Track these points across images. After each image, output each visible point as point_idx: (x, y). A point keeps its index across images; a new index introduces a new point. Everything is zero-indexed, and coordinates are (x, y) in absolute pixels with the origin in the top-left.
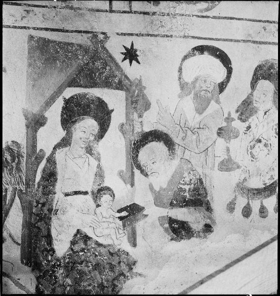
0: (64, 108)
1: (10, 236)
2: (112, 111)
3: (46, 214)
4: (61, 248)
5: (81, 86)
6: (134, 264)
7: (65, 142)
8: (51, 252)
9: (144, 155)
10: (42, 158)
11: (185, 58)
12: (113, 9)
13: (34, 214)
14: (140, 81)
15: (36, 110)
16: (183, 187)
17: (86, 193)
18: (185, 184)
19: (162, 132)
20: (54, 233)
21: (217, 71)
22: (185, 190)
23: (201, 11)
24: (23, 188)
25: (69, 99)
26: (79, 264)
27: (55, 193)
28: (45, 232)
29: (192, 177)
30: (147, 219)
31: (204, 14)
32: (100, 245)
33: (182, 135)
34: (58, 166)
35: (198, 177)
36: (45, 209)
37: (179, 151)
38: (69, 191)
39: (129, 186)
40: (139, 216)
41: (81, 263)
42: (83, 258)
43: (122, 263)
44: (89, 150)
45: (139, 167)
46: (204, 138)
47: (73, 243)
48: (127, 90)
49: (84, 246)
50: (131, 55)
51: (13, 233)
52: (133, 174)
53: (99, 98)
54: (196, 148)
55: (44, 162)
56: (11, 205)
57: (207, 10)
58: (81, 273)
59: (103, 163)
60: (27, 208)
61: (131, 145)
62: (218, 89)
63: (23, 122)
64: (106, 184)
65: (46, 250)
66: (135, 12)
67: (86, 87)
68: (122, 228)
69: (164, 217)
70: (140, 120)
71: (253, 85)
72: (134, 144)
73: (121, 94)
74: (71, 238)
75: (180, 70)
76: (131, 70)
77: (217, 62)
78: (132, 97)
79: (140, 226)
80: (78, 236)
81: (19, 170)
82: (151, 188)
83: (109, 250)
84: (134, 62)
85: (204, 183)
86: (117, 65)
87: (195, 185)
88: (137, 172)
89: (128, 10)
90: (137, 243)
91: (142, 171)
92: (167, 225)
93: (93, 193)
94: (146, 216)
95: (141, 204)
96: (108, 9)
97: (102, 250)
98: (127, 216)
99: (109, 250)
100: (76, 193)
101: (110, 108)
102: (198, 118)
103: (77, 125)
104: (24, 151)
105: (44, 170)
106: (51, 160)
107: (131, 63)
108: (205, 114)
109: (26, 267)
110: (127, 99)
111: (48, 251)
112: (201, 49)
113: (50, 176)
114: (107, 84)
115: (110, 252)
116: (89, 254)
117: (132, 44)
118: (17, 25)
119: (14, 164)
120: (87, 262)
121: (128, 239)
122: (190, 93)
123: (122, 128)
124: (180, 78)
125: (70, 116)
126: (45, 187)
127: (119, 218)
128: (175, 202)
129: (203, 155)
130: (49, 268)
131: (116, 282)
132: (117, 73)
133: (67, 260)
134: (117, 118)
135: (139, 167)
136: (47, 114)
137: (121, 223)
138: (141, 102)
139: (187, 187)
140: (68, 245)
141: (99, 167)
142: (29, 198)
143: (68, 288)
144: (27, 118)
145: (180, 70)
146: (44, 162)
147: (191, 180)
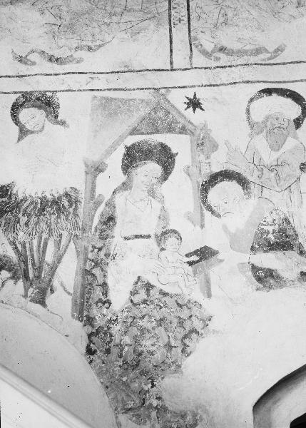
0: (125, 155)
1: (62, 285)
2: (177, 154)
3: (102, 260)
4: (119, 297)
5: (142, 134)
6: (210, 320)
7: (125, 186)
8: (107, 305)
9: (214, 195)
10: (98, 204)
11: (252, 100)
12: (174, 68)
13: (90, 260)
14: (205, 125)
15: (95, 158)
16: (265, 228)
17: (149, 236)
18: (268, 224)
19: (233, 172)
20: (110, 281)
22: (268, 233)
23: (264, 60)
24: (79, 233)
25: (130, 147)
26: (140, 318)
27: (113, 237)
28: (100, 281)
29: (274, 216)
30: (222, 265)
32: (165, 294)
33: (257, 173)
34: (117, 210)
35: (282, 216)
36: (102, 254)
37: (255, 190)
38: (129, 234)
39: (198, 228)
40: (213, 259)
41: (143, 317)
42: (145, 311)
43: (193, 318)
44: (152, 193)
45: (210, 208)
46: (284, 176)
47: (134, 293)
49: (145, 297)
50: (194, 104)
51: (65, 283)
52: (202, 215)
53: (162, 144)
54: (276, 185)
55: (103, 205)
56: (65, 251)
57: (270, 59)
58: (143, 330)
59: (167, 205)
60: (82, 254)
61: (199, 187)
62: (292, 124)
63: (83, 168)
64: (171, 227)
65: (100, 300)
66: (196, 68)
68: (192, 274)
69: (242, 264)
70: (208, 161)
72: (203, 185)
73: (185, 138)
74: (131, 288)
75: (248, 111)
76: (195, 117)
77: (289, 100)
78: (198, 139)
79: (215, 271)
80: (139, 284)
81: (76, 215)
82: (225, 228)
83: (176, 301)
84: (198, 110)
85: (292, 222)
86: (179, 113)
87: (279, 225)
88: (207, 214)
90: (212, 293)
91: (213, 212)
92: (250, 274)
93: (156, 236)
94: (221, 261)
95: (215, 248)
97: (167, 299)
98: (198, 262)
99: (176, 301)
100: (137, 237)
101: (174, 151)
102: (275, 155)
103: (139, 170)
104: (83, 196)
105: (102, 215)
106: (110, 204)
107: (194, 110)
108: (282, 150)
109: (77, 321)
110: (191, 142)
111: (104, 303)
112: (269, 92)
113: (110, 220)
114: (170, 130)
115: (178, 304)
116: (152, 306)
117: (195, 95)
118: (81, 89)
119: (71, 210)
120: (150, 316)
121: (201, 289)
122: (262, 132)
123: (188, 170)
124: (248, 119)
125: (131, 162)
126: (102, 231)
127: (188, 262)
128: (257, 246)
129: (286, 192)
130: (102, 323)
131: (186, 341)
132: (180, 120)
133: (125, 314)
134: (181, 162)
135: (210, 208)
136: (107, 162)
137: (190, 269)
138: (207, 144)
139: (270, 229)
140: (128, 295)
141: (163, 209)
142: (85, 243)
143: (126, 348)
144: (87, 166)
145: (248, 111)
146: (103, 205)
147: (274, 220)
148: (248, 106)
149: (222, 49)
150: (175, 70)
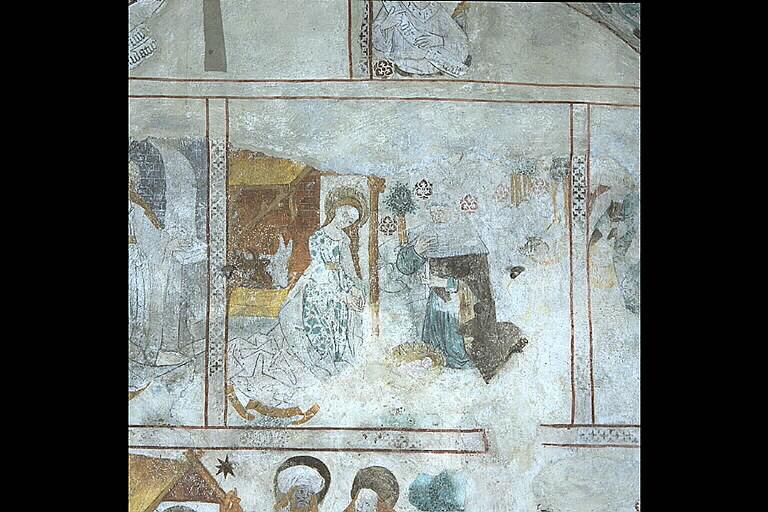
11: (279, 471)
14: (235, 493)
21: (318, 484)
31: (299, 426)
48: (222, 503)
50: (226, 468)
57: (302, 422)
66: (230, 427)
67: (180, 501)
71: (354, 495)
75: (276, 480)
77: (314, 472)
84: (229, 474)
89: (222, 425)
96: (204, 425)
107: (226, 475)
112: (297, 461)
114: (203, 499)
145: (276, 480)
148: (277, 475)
149: (256, 405)
150: (209, 427)
